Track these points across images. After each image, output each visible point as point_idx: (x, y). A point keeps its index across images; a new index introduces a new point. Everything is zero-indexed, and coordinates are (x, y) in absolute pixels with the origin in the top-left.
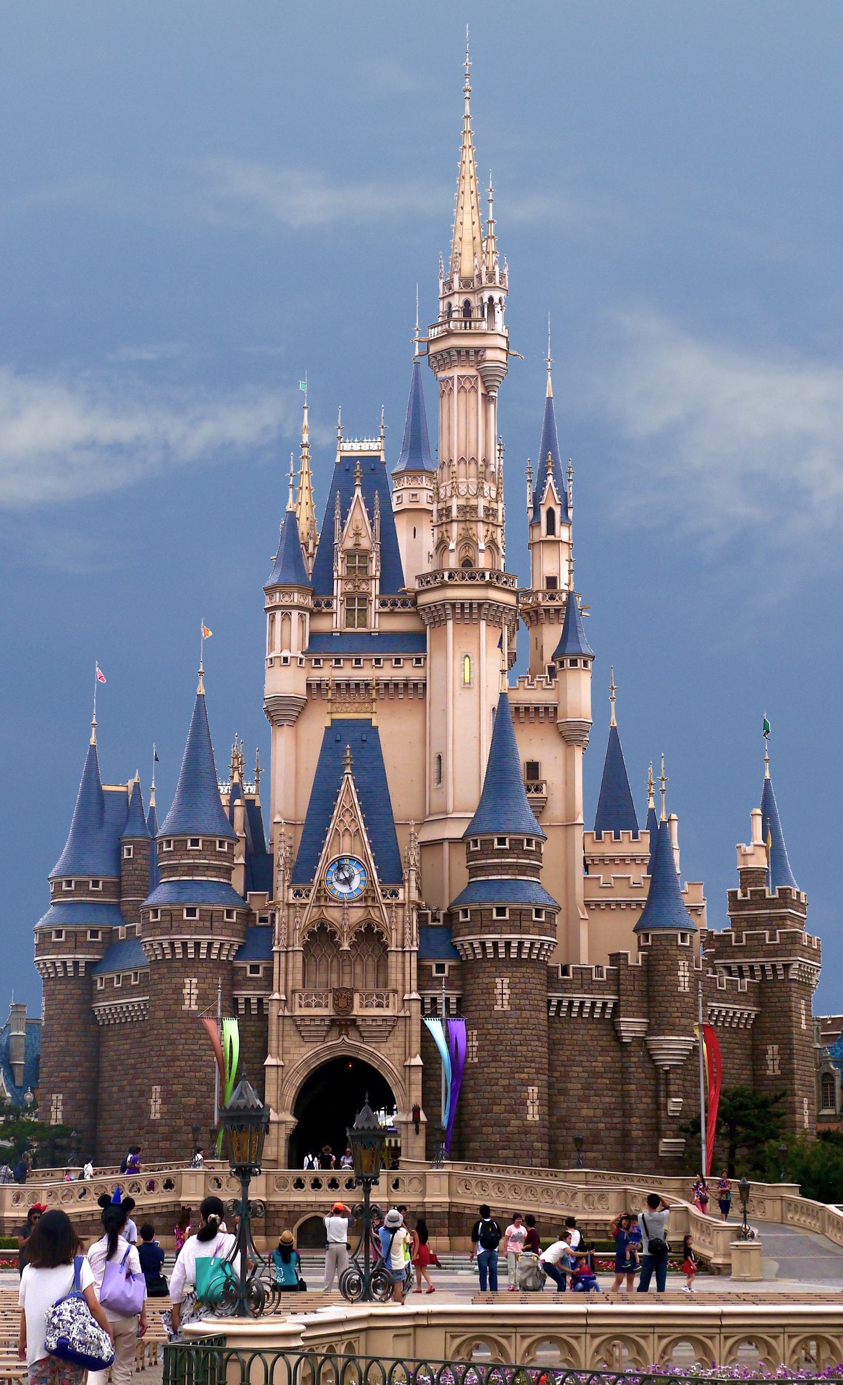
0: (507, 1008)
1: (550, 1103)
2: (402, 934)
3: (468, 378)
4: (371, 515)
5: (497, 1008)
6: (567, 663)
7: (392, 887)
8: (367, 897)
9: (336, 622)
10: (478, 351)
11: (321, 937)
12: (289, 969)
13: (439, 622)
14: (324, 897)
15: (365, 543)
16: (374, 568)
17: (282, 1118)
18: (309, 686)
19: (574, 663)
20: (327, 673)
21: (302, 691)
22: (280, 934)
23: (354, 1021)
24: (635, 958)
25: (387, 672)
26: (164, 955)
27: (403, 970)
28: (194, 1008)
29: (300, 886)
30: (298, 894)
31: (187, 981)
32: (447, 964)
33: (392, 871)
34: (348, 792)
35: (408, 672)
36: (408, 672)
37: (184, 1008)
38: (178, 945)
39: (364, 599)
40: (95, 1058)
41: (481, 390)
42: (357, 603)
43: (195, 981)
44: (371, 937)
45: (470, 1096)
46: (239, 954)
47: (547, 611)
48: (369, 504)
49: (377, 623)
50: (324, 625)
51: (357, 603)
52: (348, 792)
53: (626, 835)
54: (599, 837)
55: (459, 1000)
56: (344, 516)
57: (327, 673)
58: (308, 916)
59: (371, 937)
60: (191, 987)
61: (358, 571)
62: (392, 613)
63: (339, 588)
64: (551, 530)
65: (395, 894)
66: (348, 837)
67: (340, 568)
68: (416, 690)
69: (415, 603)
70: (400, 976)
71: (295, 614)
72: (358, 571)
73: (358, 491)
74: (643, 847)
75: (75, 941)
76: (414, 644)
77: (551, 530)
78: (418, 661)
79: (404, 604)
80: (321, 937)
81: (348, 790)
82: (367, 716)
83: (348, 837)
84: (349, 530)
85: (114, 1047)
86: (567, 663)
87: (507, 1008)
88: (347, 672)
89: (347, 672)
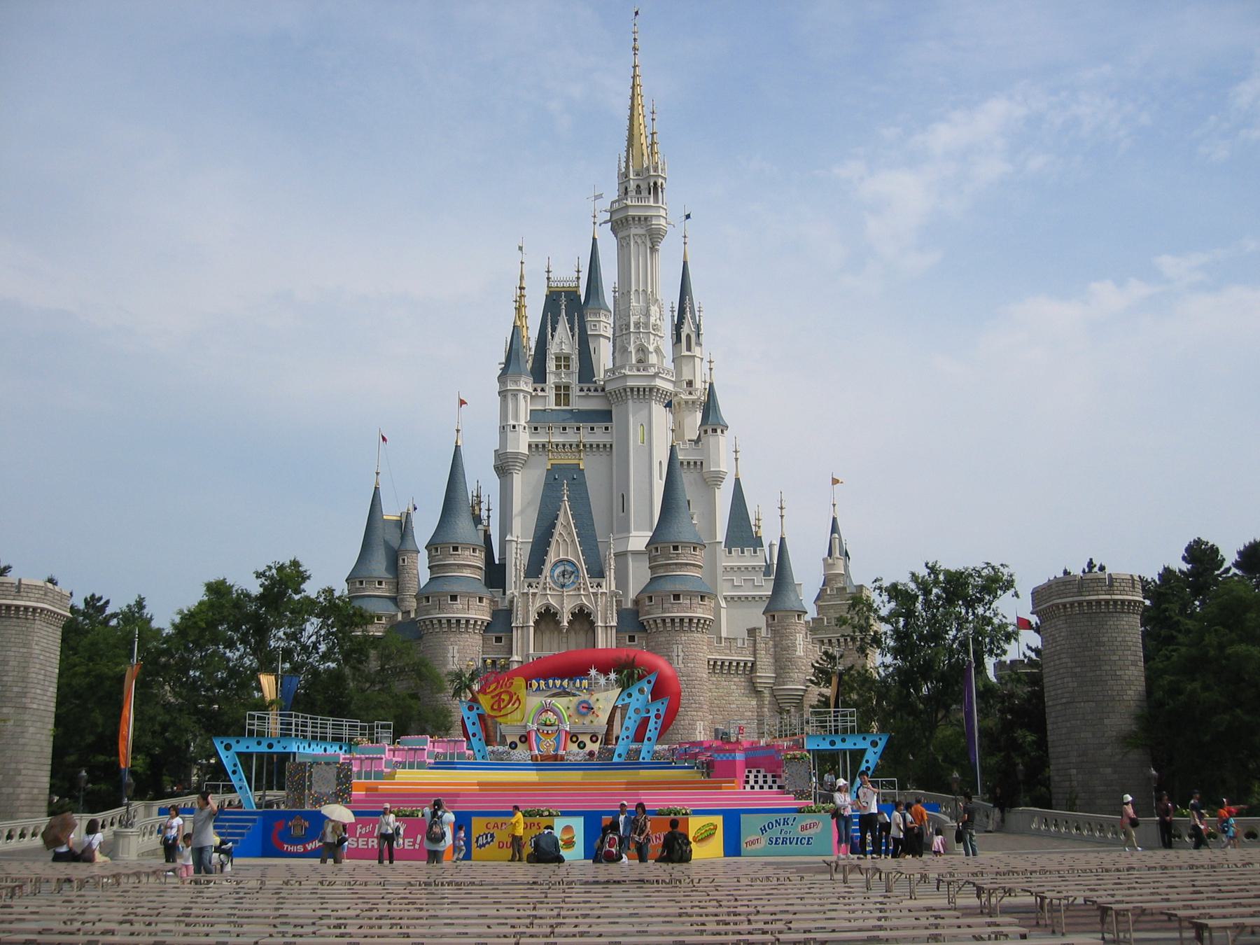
3: (640, 236)
4: (572, 329)
6: (710, 431)
7: (598, 580)
10: (646, 218)
11: (547, 617)
15: (566, 349)
16: (575, 365)
18: (530, 446)
19: (715, 431)
20: (541, 439)
21: (524, 449)
29: (531, 580)
30: (530, 585)
34: (566, 516)
35: (599, 437)
36: (599, 437)
39: (567, 388)
41: (649, 244)
47: (686, 402)
49: (577, 404)
51: (563, 393)
52: (566, 516)
53: (748, 551)
54: (730, 552)
56: (554, 329)
62: (587, 396)
63: (551, 379)
64: (689, 349)
65: (599, 585)
66: (564, 548)
67: (551, 365)
69: (603, 390)
71: (521, 395)
76: (606, 416)
77: (689, 349)
78: (607, 429)
79: (596, 390)
80: (547, 617)
81: (566, 512)
82: (576, 462)
84: (556, 339)
86: (710, 431)
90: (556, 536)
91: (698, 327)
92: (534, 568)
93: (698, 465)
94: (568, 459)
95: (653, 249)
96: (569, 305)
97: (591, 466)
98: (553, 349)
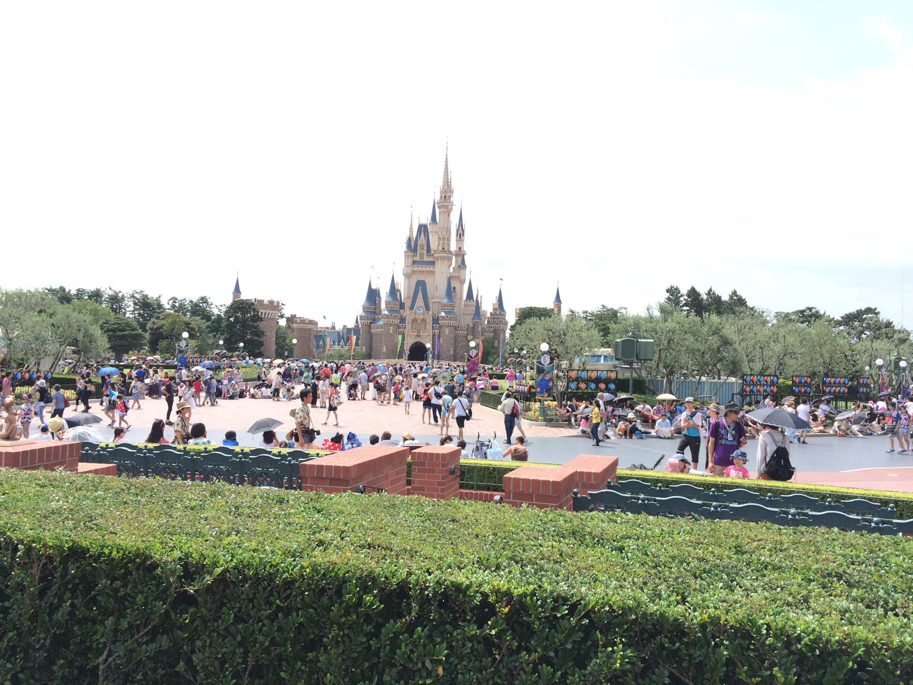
1: (455, 351)
2: (429, 320)
8: (424, 314)
9: (417, 259)
12: (408, 325)
13: (437, 260)
14: (415, 313)
17: (407, 352)
20: (416, 269)
24: (471, 325)
25: (427, 269)
27: (429, 327)
33: (428, 309)
34: (420, 295)
35: (431, 269)
40: (371, 340)
42: (422, 255)
44: (424, 320)
49: (426, 259)
50: (415, 259)
51: (422, 255)
52: (420, 295)
57: (416, 269)
58: (413, 317)
59: (424, 320)
60: (391, 328)
61: (422, 248)
68: (433, 272)
72: (422, 248)
74: (475, 303)
75: (367, 318)
76: (433, 263)
80: (415, 320)
83: (420, 302)
85: (375, 338)
88: (420, 269)
89: (420, 269)
91: (463, 231)
92: (412, 308)
93: (458, 277)
94: (421, 278)
95: (449, 215)
96: (423, 228)
97: (428, 281)
98: (420, 242)
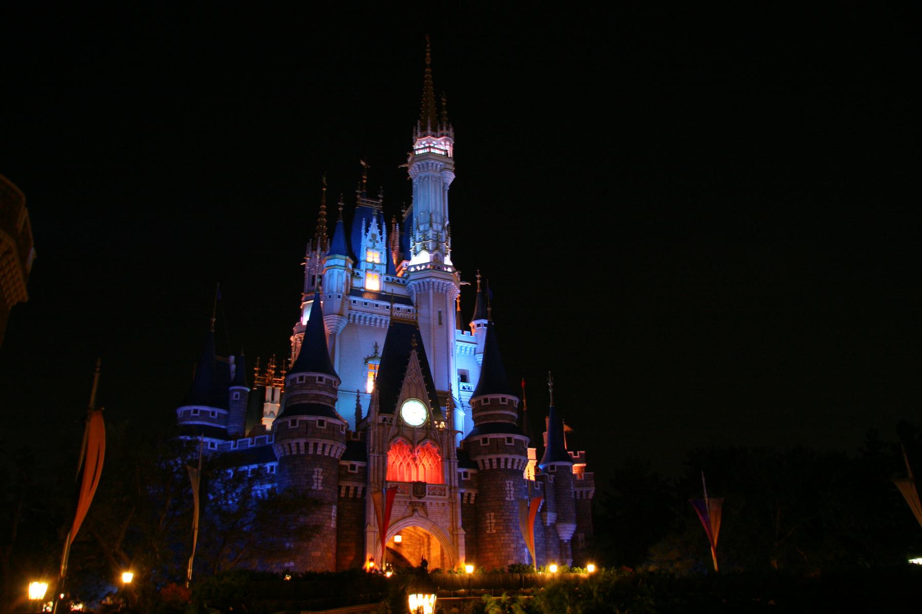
0: (513, 499)
4: (381, 233)
5: (507, 499)
22: (374, 445)
23: (424, 504)
26: (298, 450)
28: (320, 488)
31: (316, 470)
32: (470, 471)
37: (313, 488)
38: (311, 445)
43: (321, 470)
45: (490, 554)
46: (345, 457)
48: (380, 227)
55: (476, 497)
56: (367, 231)
70: (448, 477)
73: (374, 220)
87: (513, 499)
90: (408, 378)
